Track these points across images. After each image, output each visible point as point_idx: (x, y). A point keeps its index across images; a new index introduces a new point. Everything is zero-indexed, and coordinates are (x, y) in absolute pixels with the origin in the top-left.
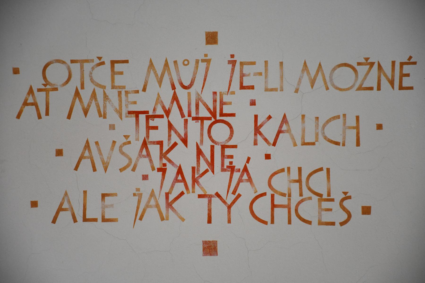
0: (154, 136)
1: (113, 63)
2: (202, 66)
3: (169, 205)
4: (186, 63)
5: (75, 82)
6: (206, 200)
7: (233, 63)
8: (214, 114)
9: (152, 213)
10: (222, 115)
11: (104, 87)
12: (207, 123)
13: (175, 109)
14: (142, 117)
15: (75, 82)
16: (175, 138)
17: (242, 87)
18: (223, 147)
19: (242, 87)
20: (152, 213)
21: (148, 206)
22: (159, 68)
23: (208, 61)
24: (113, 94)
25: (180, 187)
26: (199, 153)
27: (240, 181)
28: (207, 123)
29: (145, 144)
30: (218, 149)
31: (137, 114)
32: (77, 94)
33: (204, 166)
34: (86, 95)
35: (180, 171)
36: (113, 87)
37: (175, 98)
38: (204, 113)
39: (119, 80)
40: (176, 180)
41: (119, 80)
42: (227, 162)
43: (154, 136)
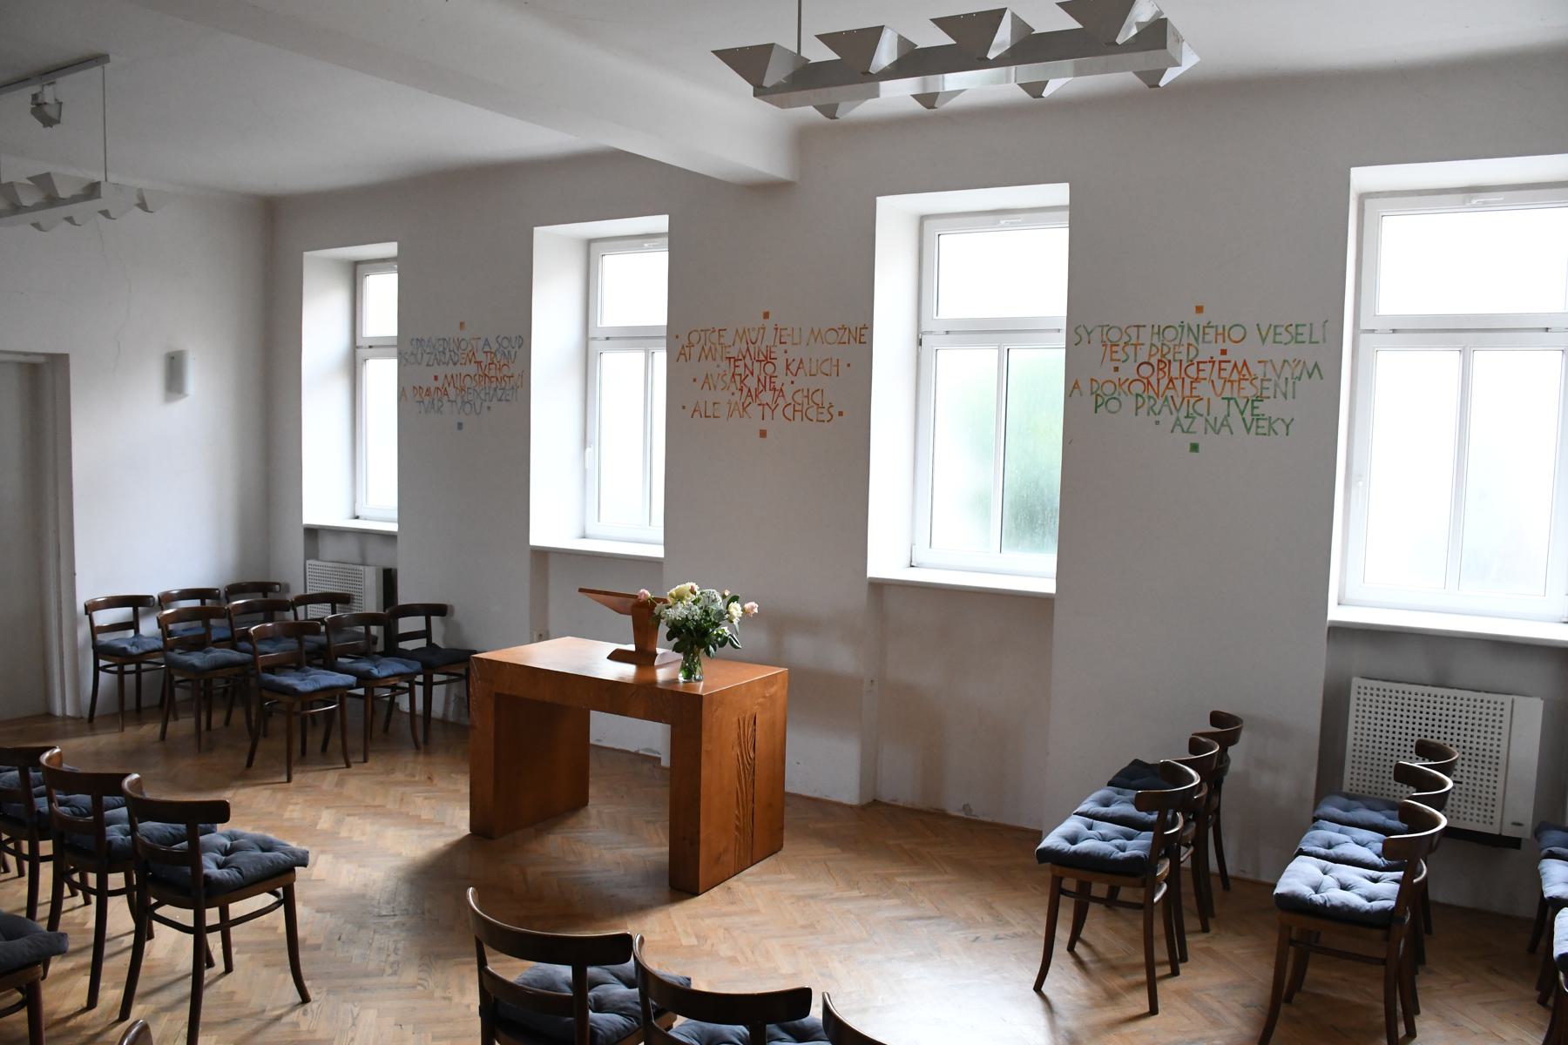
0: (738, 371)
2: (762, 331)
3: (744, 409)
5: (702, 341)
8: (766, 358)
9: (736, 414)
11: (714, 344)
12: (763, 363)
13: (748, 355)
14: (732, 360)
15: (702, 341)
16: (747, 372)
17: (781, 343)
18: (771, 377)
19: (781, 343)
20: (736, 414)
22: (741, 332)
23: (764, 328)
24: (719, 347)
25: (749, 400)
26: (759, 380)
27: (779, 396)
28: (763, 363)
31: (730, 358)
32: (703, 348)
33: (761, 388)
34: (706, 348)
35: (749, 391)
37: (748, 349)
38: (762, 358)
39: (722, 340)
41: (722, 340)
42: (772, 386)
43: (738, 371)
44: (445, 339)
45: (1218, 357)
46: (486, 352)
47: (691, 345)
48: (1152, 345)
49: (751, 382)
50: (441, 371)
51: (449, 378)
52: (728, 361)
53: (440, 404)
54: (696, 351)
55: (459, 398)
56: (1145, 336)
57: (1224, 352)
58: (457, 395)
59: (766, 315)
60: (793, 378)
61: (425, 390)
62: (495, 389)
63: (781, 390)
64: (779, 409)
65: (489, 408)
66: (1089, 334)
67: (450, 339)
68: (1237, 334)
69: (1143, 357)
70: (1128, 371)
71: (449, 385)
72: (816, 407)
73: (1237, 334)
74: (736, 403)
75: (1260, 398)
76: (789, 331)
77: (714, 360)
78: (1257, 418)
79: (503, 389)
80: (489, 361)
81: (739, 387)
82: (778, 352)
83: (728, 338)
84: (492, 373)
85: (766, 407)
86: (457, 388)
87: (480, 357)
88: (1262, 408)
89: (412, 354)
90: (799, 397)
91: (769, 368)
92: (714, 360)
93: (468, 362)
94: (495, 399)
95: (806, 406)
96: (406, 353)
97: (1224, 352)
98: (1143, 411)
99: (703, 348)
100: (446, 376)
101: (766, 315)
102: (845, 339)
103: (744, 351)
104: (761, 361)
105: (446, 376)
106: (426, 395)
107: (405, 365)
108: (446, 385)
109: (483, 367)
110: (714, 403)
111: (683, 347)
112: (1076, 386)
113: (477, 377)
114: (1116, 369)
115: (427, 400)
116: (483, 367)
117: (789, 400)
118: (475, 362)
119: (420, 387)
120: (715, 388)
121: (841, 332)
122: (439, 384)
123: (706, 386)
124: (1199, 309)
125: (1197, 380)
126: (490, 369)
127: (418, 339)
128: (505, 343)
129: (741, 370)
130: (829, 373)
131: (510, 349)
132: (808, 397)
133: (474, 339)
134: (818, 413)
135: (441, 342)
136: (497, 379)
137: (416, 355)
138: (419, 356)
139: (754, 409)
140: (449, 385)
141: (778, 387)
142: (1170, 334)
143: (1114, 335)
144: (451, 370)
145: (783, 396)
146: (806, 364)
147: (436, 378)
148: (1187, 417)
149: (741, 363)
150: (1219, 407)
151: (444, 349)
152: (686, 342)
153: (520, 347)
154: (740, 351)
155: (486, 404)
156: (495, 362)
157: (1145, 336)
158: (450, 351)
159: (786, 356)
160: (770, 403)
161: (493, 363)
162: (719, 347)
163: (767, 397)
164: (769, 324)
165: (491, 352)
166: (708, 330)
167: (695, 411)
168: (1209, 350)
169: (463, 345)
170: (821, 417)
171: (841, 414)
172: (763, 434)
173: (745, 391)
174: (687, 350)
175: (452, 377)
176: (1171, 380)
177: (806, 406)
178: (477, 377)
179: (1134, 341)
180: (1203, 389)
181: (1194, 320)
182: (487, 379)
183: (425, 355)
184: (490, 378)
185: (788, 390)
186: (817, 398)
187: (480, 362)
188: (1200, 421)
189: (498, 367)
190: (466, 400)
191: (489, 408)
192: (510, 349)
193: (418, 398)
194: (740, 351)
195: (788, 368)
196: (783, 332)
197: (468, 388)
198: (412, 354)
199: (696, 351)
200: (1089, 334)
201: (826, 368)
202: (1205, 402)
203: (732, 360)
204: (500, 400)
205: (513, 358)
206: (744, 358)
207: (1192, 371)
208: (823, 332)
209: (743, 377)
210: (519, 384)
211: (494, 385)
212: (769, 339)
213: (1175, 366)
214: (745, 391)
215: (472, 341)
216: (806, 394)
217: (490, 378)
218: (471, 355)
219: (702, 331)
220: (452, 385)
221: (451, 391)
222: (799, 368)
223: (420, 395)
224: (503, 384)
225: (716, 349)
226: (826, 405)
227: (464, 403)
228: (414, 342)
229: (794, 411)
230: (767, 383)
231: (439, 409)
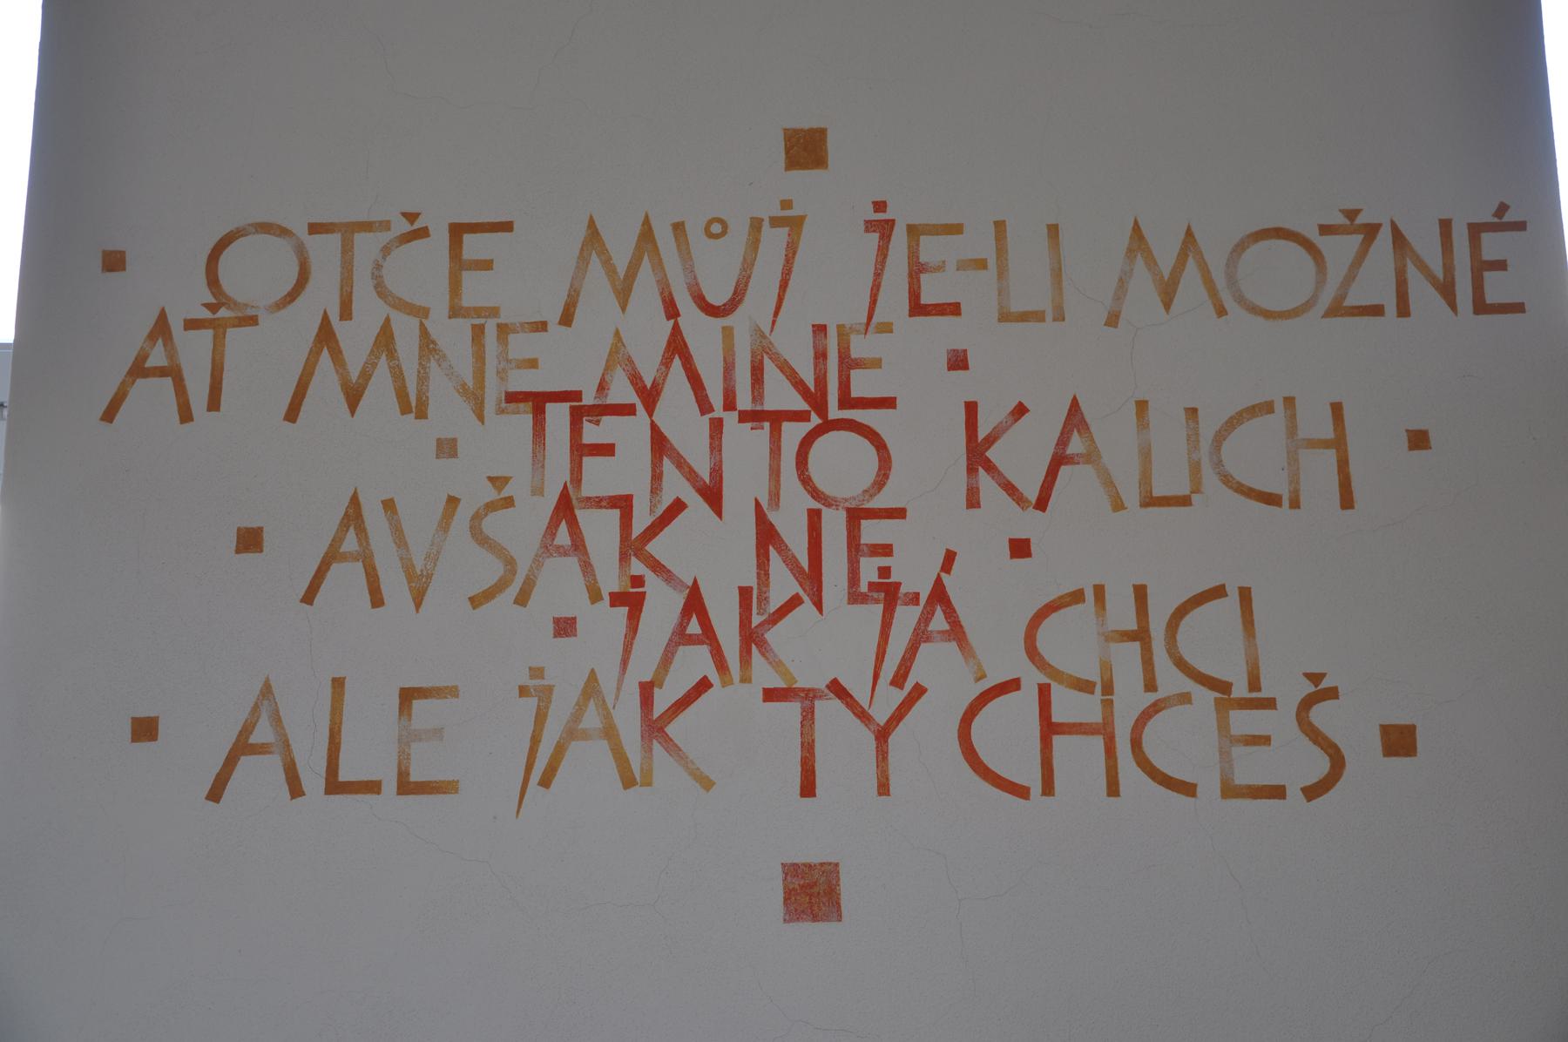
1: (458, 231)
2: (774, 241)
3: (654, 728)
4: (717, 229)
5: (322, 295)
6: (791, 711)
7: (884, 229)
10: (846, 401)
11: (422, 312)
12: (793, 433)
13: (677, 385)
14: (558, 415)
15: (322, 295)
16: (675, 485)
17: (918, 308)
18: (856, 516)
19: (918, 308)
21: (572, 733)
22: (621, 249)
23: (795, 224)
24: (453, 336)
25: (694, 662)
26: (767, 536)
27: (920, 636)
28: (793, 433)
29: (565, 508)
30: (834, 525)
31: (538, 402)
32: (326, 335)
33: (783, 585)
34: (356, 339)
35: (694, 604)
36: (456, 312)
37: (677, 347)
38: (781, 396)
39: (476, 289)
40: (681, 637)
41: (476, 289)
42: (869, 569)
43: (600, 477)
52: (523, 420)
60: (1027, 524)
63: (939, 595)
72: (1205, 698)
74: (591, 687)
81: (611, 581)
85: (829, 710)
92: (414, 406)
95: (1130, 699)
99: (326, 335)
102: (1375, 285)
103: (648, 361)
104: (777, 419)
111: (161, 328)
117: (1006, 661)
121: (1340, 249)
123: (346, 579)
130: (1280, 487)
132: (1141, 635)
134: (1228, 739)
141: (915, 575)
145: (956, 631)
152: (191, 299)
154: (618, 354)
159: (963, 386)
166: (367, 226)
167: (242, 747)
171: (1399, 741)
173: (663, 605)
177: (1130, 699)
194: (618, 354)
195: (977, 455)
196: (931, 249)
203: (558, 415)
206: (650, 396)
209: (639, 526)
214: (663, 605)
216: (1122, 615)
219: (315, 229)
222: (1059, 460)
225: (428, 345)
226: (1288, 689)
229: (1049, 729)
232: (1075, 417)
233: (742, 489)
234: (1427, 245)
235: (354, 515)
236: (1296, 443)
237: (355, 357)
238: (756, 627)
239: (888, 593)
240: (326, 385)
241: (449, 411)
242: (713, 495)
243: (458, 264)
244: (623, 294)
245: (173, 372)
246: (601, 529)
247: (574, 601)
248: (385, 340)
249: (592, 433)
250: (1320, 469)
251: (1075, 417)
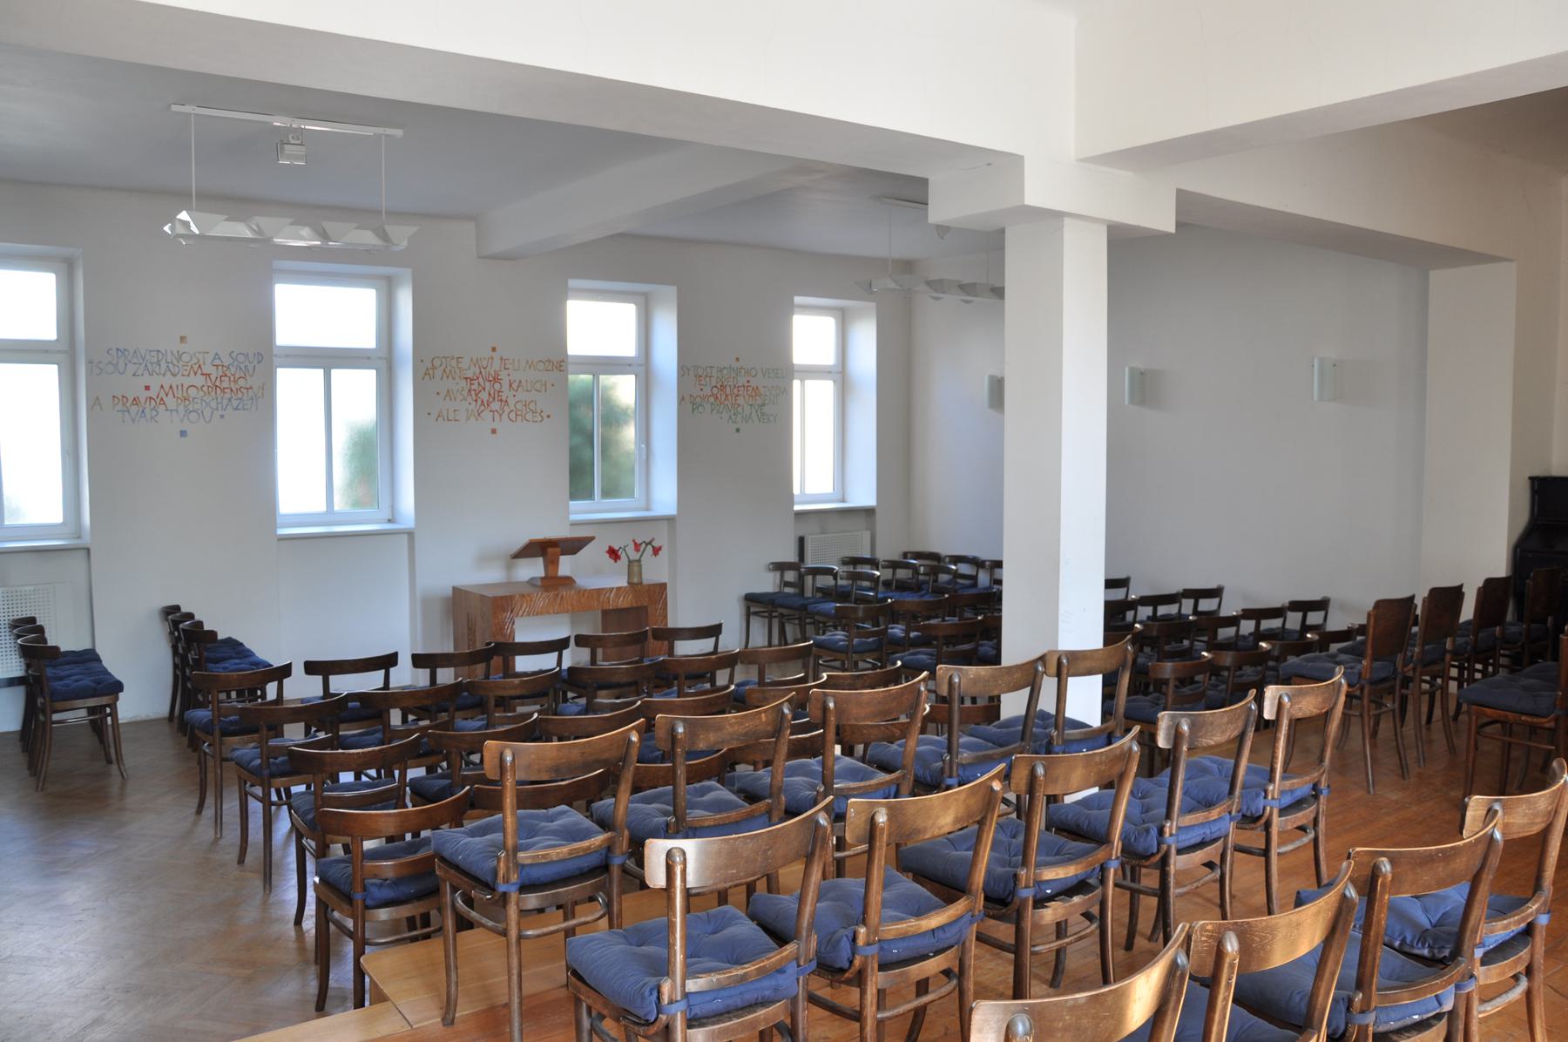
0: (473, 387)
2: (490, 360)
3: (479, 415)
7: (501, 359)
9: (472, 419)
11: (454, 368)
13: (481, 379)
14: (469, 380)
15: (444, 366)
16: (480, 388)
20: (472, 419)
23: (492, 358)
24: (458, 371)
25: (483, 408)
26: (490, 394)
31: (466, 378)
35: (482, 402)
38: (491, 379)
39: (460, 365)
41: (460, 365)
43: (473, 387)
44: (158, 351)
45: (746, 384)
46: (217, 366)
47: (434, 368)
48: (717, 377)
49: (484, 396)
50: (155, 382)
51: (167, 388)
53: (154, 413)
54: (438, 372)
55: (181, 409)
56: (714, 370)
57: (748, 382)
58: (178, 405)
59: (494, 349)
61: (130, 402)
62: (230, 400)
64: (506, 413)
65: (222, 416)
66: (688, 370)
67: (166, 351)
68: (753, 373)
69: (714, 384)
70: (707, 391)
71: (167, 395)
73: (753, 373)
75: (763, 405)
76: (511, 361)
77: (454, 379)
78: (763, 414)
79: (241, 399)
80: (221, 374)
81: (474, 398)
82: (503, 375)
83: (465, 364)
84: (225, 385)
86: (178, 398)
87: (207, 369)
88: (766, 409)
89: (110, 363)
90: (519, 406)
91: (497, 386)
92: (454, 379)
93: (192, 374)
94: (230, 409)
95: (524, 412)
96: (100, 362)
97: (748, 382)
98: (714, 412)
100: (162, 386)
101: (494, 349)
102: (550, 368)
103: (477, 372)
105: (162, 386)
106: (132, 404)
107: (98, 375)
108: (162, 394)
109: (213, 380)
110: (455, 411)
111: (427, 369)
112: (683, 399)
113: (205, 389)
114: (702, 390)
115: (134, 409)
116: (213, 380)
117: (512, 408)
118: (202, 374)
119: (123, 397)
120: (455, 399)
122: (153, 393)
123: (448, 398)
124: (737, 359)
125: (737, 396)
126: (221, 381)
127: (118, 349)
128: (241, 358)
129: (475, 387)
131: (247, 363)
133: (200, 353)
135: (154, 354)
136: (232, 390)
137: (116, 366)
138: (121, 367)
139: (487, 415)
140: (167, 395)
141: (504, 399)
142: (725, 372)
143: (700, 372)
144: (168, 381)
146: (524, 383)
147: (147, 388)
148: (735, 414)
149: (476, 382)
150: (747, 408)
151: (158, 361)
152: (430, 366)
153: (259, 362)
155: (220, 412)
156: (228, 375)
157: (714, 370)
158: (167, 362)
160: (498, 409)
161: (226, 376)
162: (458, 371)
163: (496, 405)
164: (496, 355)
165: (223, 366)
167: (439, 416)
168: (742, 381)
169: (185, 358)
170: (535, 419)
171: (548, 416)
172: (494, 431)
173: (479, 402)
174: (431, 371)
175: (171, 387)
176: (726, 396)
177: (524, 412)
178: (205, 389)
179: (709, 374)
180: (740, 400)
181: (736, 365)
182: (218, 389)
183: (129, 365)
184: (223, 390)
185: (511, 401)
186: (532, 406)
187: (209, 375)
188: (739, 418)
189: (232, 379)
190: (191, 409)
191: (222, 416)
192: (247, 363)
193: (119, 407)
195: (510, 385)
197: (194, 399)
198: (110, 363)
199: (438, 372)
200: (688, 370)
201: (538, 386)
202: (741, 407)
204: (237, 409)
205: (251, 373)
206: (478, 378)
207: (735, 391)
208: (535, 363)
210: (260, 395)
211: (228, 396)
212: (497, 365)
213: (728, 388)
214: (479, 402)
215: (197, 355)
217: (223, 390)
218: (196, 367)
219: (444, 357)
220: (171, 395)
221: (170, 401)
223: (124, 404)
224: (240, 395)
225: (455, 372)
227: (188, 412)
228: (114, 352)
230: (496, 396)
231: (152, 418)
232: (520, 382)
233: (487, 389)
234: (555, 363)
235: (448, 391)
236: (541, 385)
237: (448, 373)
238: (179, 220)
239: (501, 400)
240: (445, 378)
241: (457, 378)
242: (484, 389)
243: (458, 362)
244: (475, 366)
245: (429, 374)
246: (473, 392)
247: (471, 401)
248: (450, 371)
249: (472, 382)
250: (544, 388)
251: (520, 382)
